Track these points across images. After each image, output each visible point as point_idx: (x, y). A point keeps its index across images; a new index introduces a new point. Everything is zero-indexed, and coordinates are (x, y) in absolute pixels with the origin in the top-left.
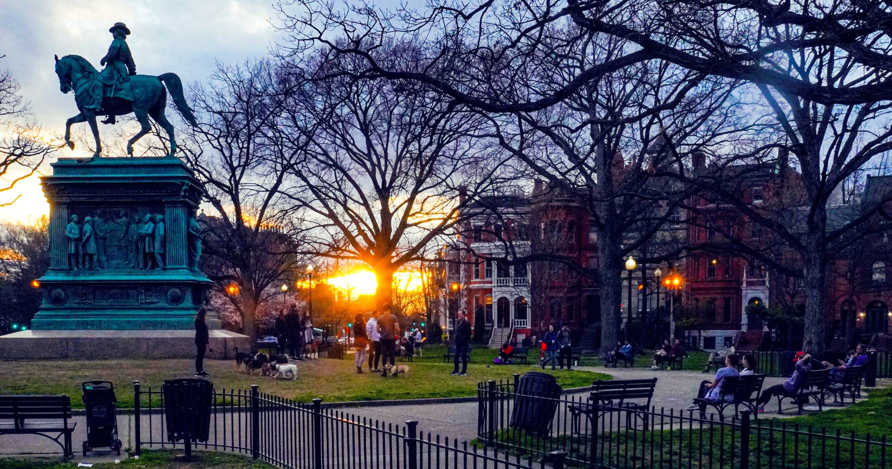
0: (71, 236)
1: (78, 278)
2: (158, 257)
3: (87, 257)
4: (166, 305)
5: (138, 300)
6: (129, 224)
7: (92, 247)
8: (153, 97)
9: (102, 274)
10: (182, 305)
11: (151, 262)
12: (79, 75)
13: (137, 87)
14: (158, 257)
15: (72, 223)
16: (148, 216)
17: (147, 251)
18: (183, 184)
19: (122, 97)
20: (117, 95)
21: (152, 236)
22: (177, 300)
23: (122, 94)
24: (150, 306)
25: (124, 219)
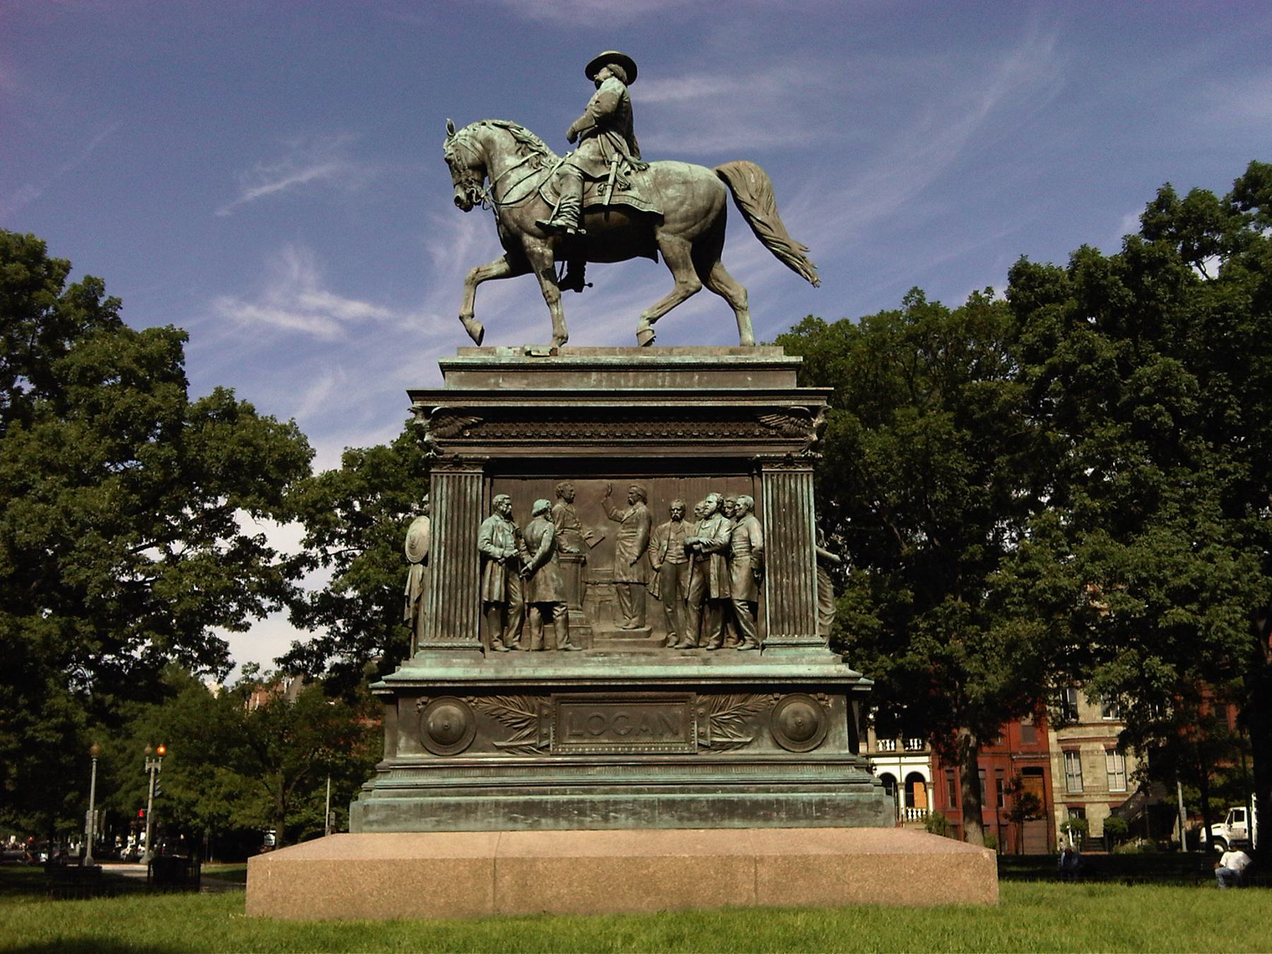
0: (496, 551)
1: (508, 673)
2: (744, 611)
3: (535, 613)
4: (780, 754)
5: (688, 740)
6: (651, 522)
7: (549, 586)
8: (708, 211)
9: (583, 663)
10: (819, 754)
11: (722, 620)
12: (512, 161)
13: (667, 185)
14: (744, 611)
15: (495, 517)
16: (713, 498)
17: (714, 594)
18: (815, 411)
19: (634, 203)
20: (616, 201)
21: (726, 551)
22: (807, 735)
23: (632, 198)
24: (731, 754)
25: (641, 508)
